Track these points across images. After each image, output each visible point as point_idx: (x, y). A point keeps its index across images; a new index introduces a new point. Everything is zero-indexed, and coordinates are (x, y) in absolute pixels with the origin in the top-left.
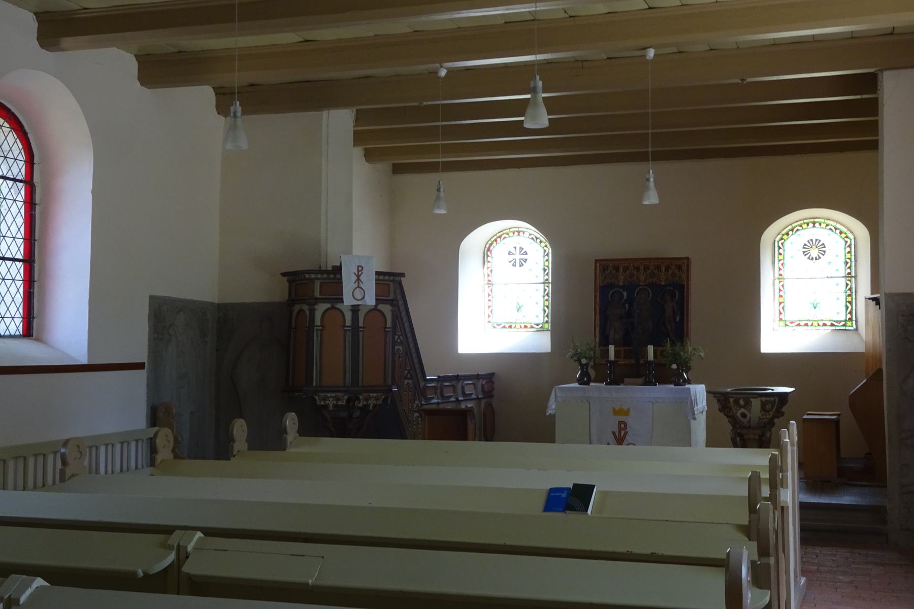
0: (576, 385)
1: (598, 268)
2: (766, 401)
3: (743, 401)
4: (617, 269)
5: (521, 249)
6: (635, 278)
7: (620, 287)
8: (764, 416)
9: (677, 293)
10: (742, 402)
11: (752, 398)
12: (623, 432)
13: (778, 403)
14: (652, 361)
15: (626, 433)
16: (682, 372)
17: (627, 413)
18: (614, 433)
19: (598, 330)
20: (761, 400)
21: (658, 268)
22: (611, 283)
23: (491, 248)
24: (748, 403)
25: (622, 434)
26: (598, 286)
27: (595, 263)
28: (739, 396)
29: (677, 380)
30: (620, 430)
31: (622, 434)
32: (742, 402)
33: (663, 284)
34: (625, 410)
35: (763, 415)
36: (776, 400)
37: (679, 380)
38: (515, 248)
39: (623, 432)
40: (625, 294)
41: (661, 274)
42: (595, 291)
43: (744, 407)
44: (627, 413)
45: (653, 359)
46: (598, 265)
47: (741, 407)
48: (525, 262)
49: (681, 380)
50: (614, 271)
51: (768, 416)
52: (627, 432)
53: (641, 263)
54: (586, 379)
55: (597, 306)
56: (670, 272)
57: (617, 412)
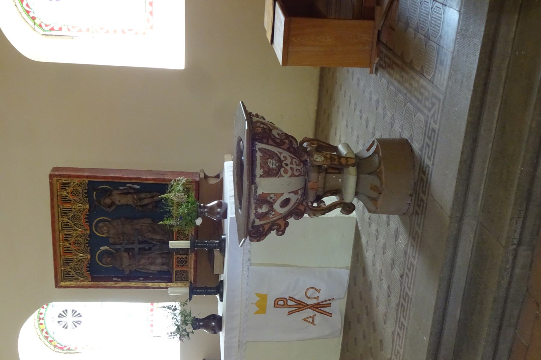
0: (222, 335)
1: (68, 284)
2: (262, 167)
3: (261, 207)
4: (68, 261)
5: (60, 316)
6: (81, 239)
7: (93, 256)
8: (288, 168)
9: (95, 197)
10: (264, 209)
11: (256, 192)
12: (290, 303)
13: (267, 143)
14: (191, 243)
15: (291, 299)
16: (205, 207)
17: (263, 298)
18: (290, 313)
19: (150, 284)
20: (261, 176)
21: (65, 213)
22: (87, 267)
23: (59, 346)
24: (264, 200)
25: (293, 303)
26: (91, 283)
27: (61, 287)
28: (253, 212)
29: (218, 216)
30: (285, 305)
31: (293, 303)
32: (264, 209)
33: (88, 206)
34: (258, 299)
35: (286, 172)
36: (260, 149)
37: (218, 213)
38: (59, 322)
39: (290, 303)
40: (102, 248)
41: (75, 209)
42: (98, 287)
43: (271, 205)
44: (263, 298)
45: (189, 241)
46: (63, 284)
47: (272, 209)
48: (76, 312)
49: (219, 210)
50: (71, 264)
51: (288, 161)
52: (290, 297)
53: (60, 232)
54: (213, 323)
55: (118, 285)
56: (70, 197)
57: (262, 308)
